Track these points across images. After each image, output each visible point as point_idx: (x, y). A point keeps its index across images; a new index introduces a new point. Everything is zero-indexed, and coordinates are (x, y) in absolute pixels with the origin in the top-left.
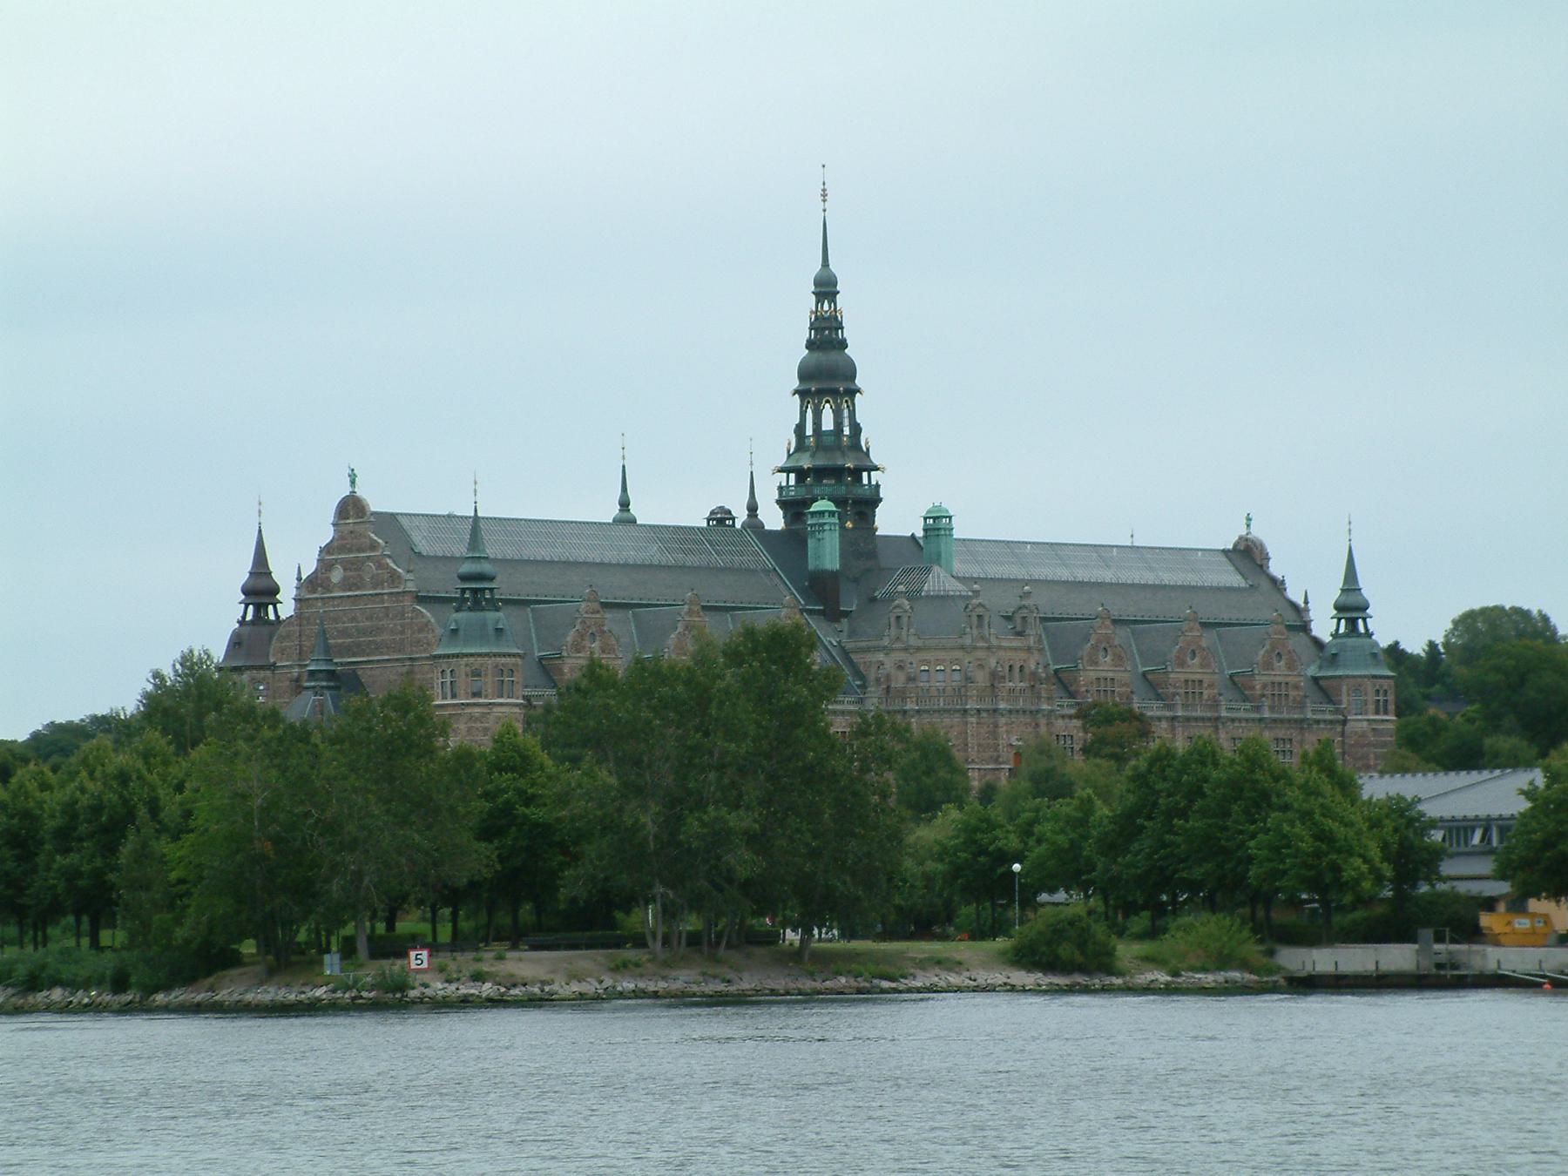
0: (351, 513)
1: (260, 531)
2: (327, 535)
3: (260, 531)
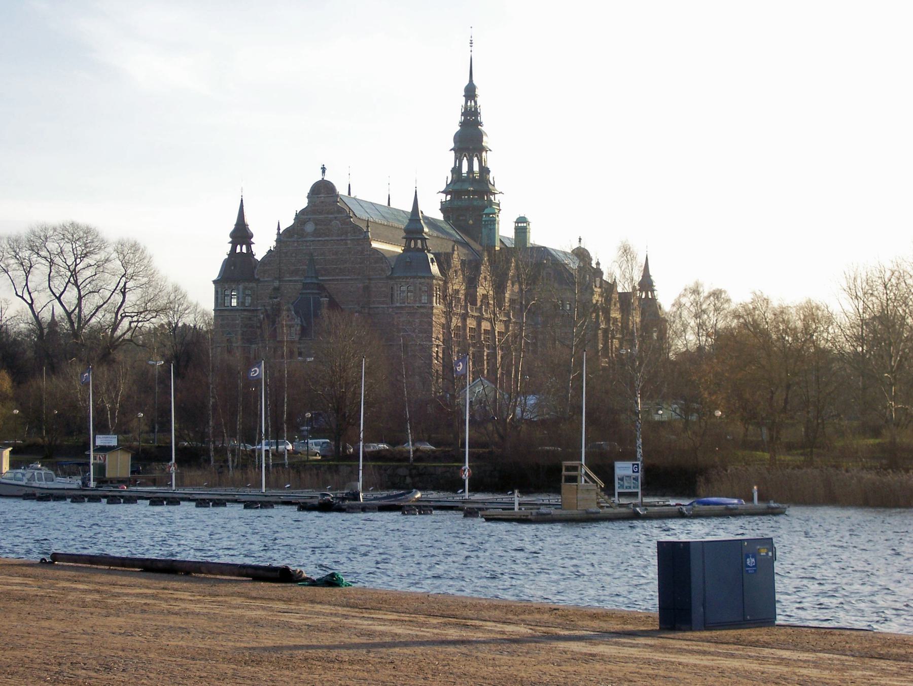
0: (323, 191)
2: (303, 203)
3: (242, 200)
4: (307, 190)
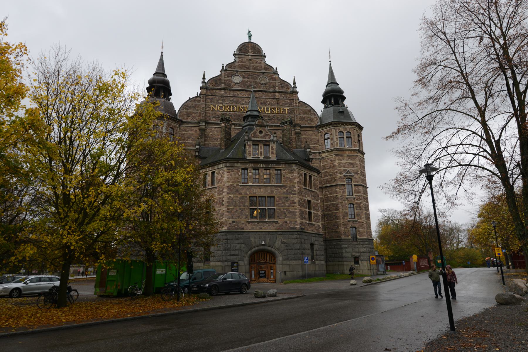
0: (250, 51)
1: (162, 55)
2: (231, 59)
3: (162, 55)
4: (235, 48)
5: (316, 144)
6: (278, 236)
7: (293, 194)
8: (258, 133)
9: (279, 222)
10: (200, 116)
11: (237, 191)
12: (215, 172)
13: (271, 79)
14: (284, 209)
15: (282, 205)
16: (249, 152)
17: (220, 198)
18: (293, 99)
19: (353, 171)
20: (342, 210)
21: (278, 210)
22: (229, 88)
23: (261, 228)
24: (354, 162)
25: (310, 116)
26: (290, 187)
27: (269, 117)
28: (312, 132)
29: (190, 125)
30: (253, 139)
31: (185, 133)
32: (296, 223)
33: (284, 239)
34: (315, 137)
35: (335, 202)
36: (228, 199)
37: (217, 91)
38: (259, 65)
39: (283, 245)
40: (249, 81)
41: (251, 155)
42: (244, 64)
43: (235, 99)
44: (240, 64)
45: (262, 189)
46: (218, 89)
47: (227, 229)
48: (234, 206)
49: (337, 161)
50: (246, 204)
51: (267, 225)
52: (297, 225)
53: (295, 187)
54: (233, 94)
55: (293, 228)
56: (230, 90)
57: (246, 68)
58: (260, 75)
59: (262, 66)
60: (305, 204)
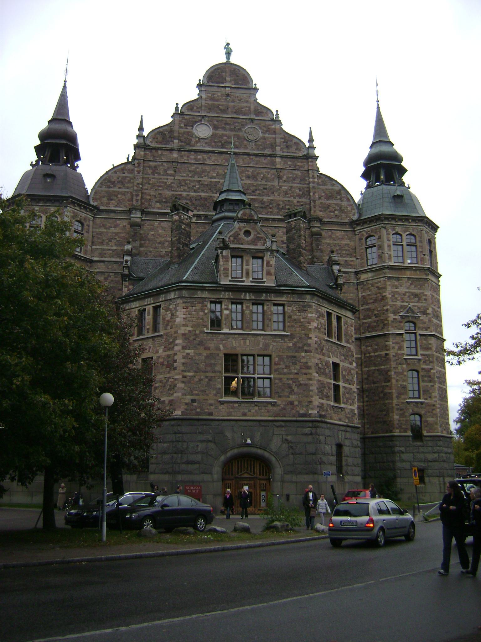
0: (228, 79)
1: (65, 87)
3: (65, 87)
4: (200, 74)
5: (350, 255)
6: (275, 429)
7: (306, 351)
8: (242, 235)
9: (279, 402)
10: (131, 200)
11: (201, 343)
12: (159, 306)
13: (267, 131)
14: (288, 379)
15: (285, 370)
16: (224, 269)
17: (168, 356)
18: (308, 171)
19: (419, 308)
20: (397, 381)
21: (277, 381)
22: (187, 147)
23: (244, 414)
24: (422, 291)
25: (339, 202)
26: (300, 338)
27: (262, 202)
28: (343, 233)
29: (112, 216)
30: (232, 246)
31: (105, 231)
32: (311, 406)
33: (287, 435)
34: (347, 242)
35: (383, 367)
36: (184, 358)
37: (166, 153)
38: (245, 105)
39: (285, 446)
40: (226, 136)
41: (227, 276)
42: (216, 103)
43: (199, 168)
44: (210, 102)
45: (248, 341)
46: (166, 150)
47: (182, 415)
48: (195, 372)
49: (389, 289)
50: (217, 369)
51: (257, 408)
52: (312, 409)
53: (310, 338)
54: (196, 159)
55: (304, 415)
56: (190, 151)
57: (221, 110)
58: (246, 124)
59: (250, 108)
60: (327, 371)
